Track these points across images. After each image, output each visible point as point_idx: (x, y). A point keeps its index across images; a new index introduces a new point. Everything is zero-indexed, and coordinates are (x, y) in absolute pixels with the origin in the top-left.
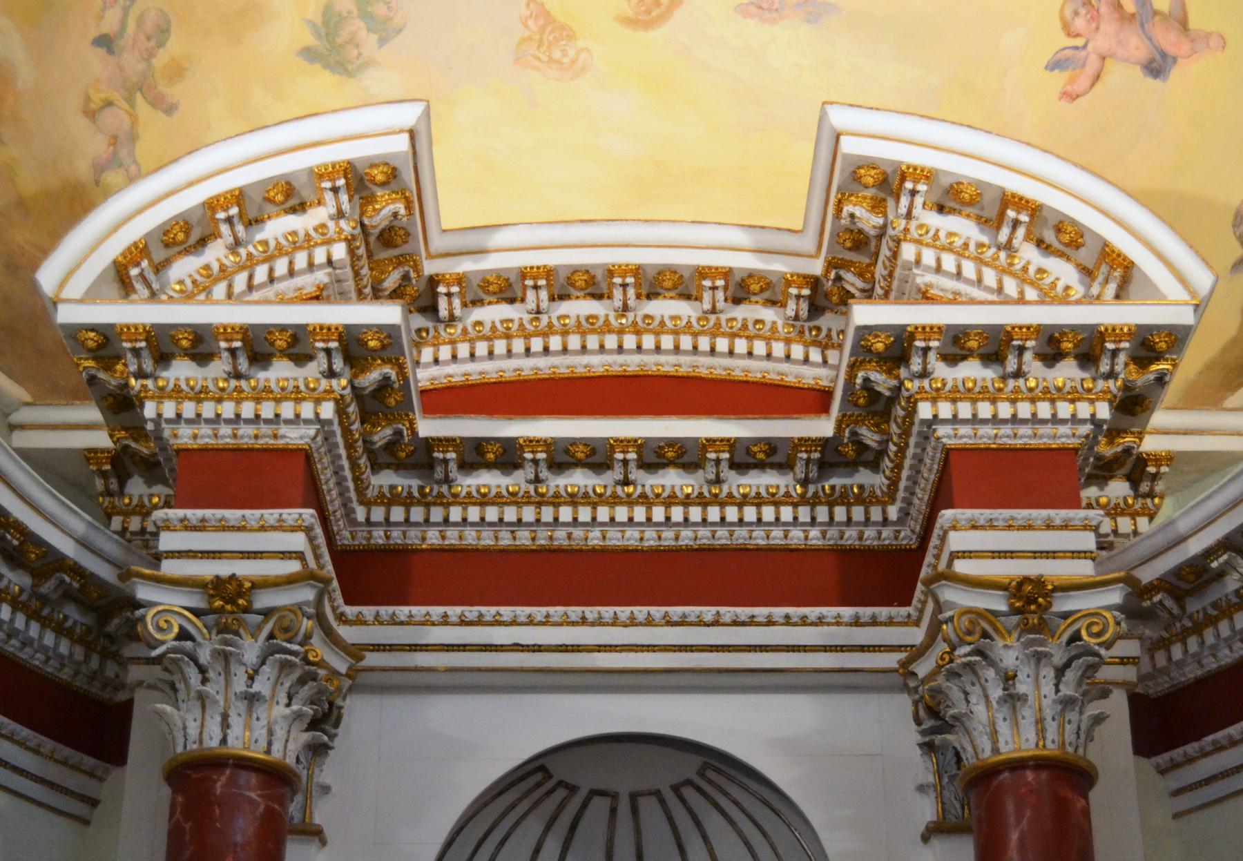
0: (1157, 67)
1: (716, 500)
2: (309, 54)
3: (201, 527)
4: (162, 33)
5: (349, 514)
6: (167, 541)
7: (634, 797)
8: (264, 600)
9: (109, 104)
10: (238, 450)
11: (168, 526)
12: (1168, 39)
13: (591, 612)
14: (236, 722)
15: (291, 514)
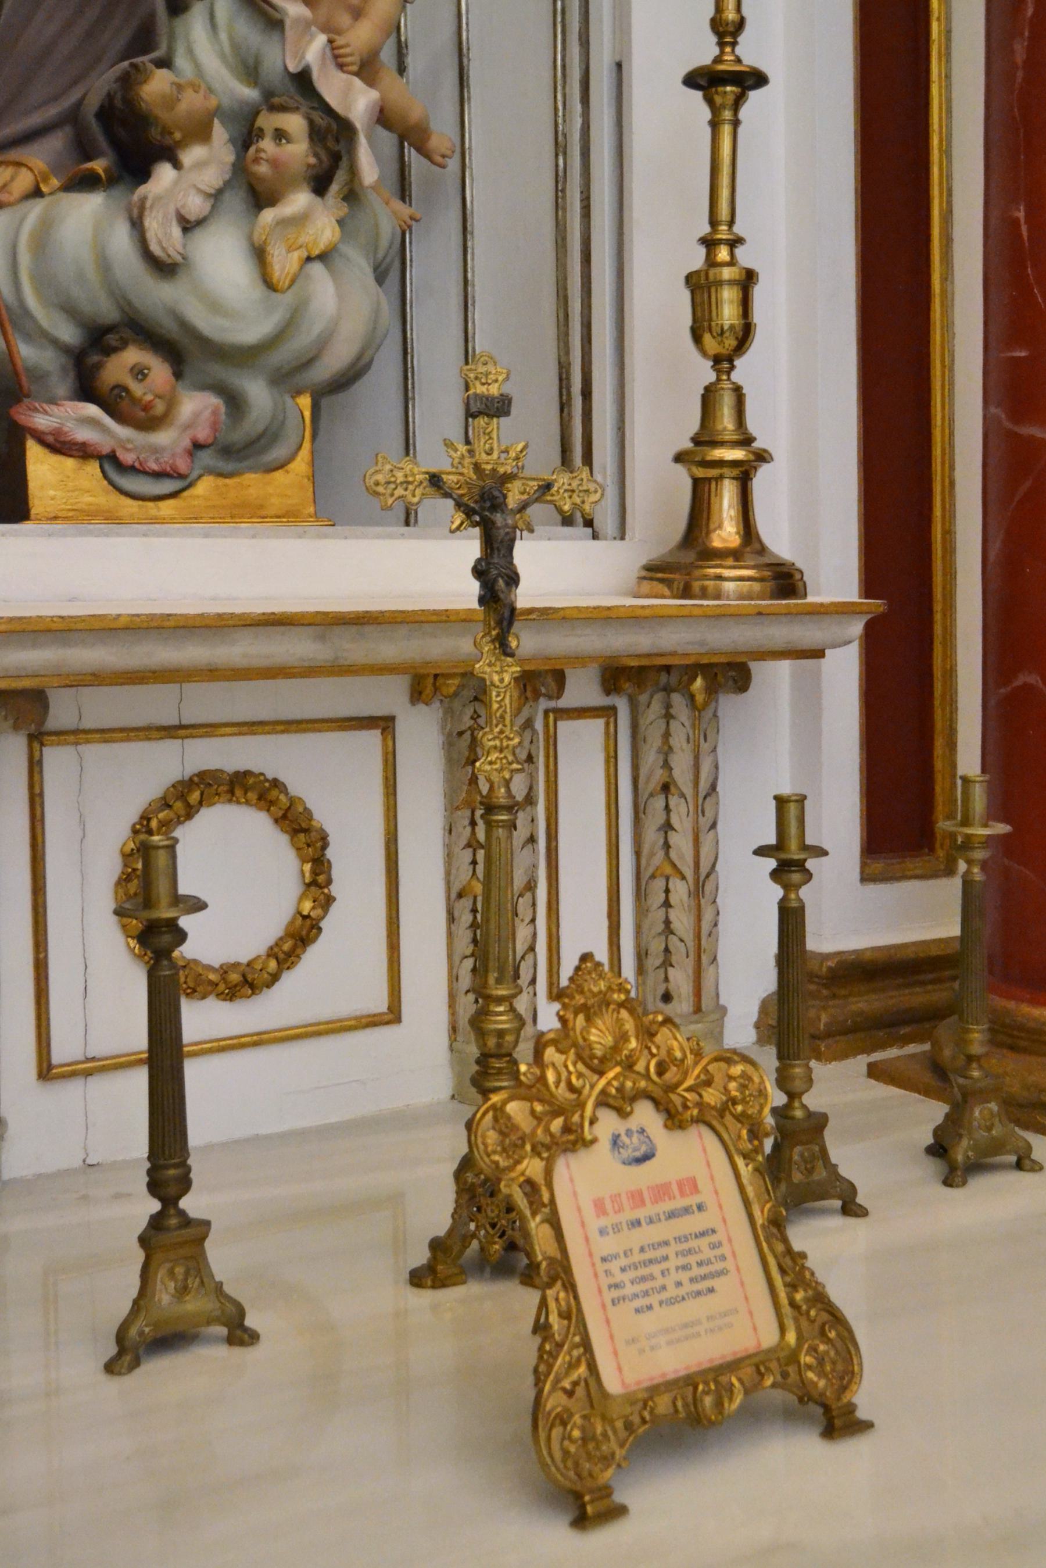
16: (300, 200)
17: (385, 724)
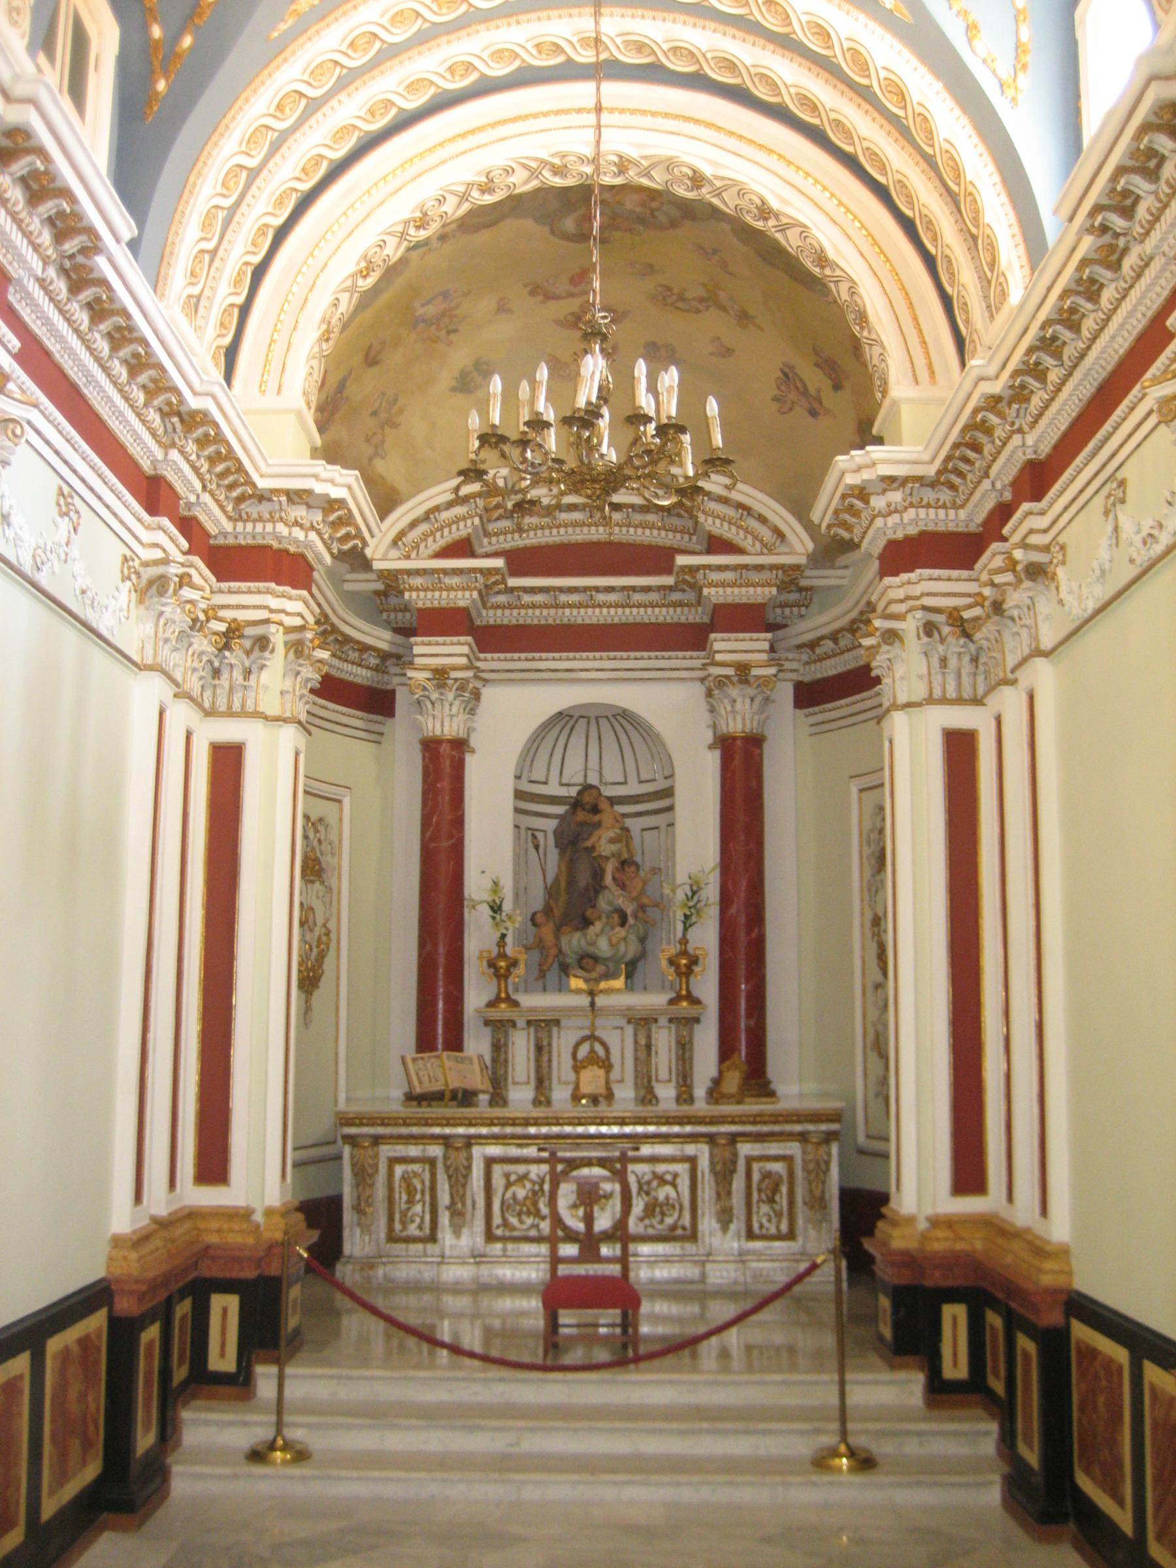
0: (813, 413)
1: (628, 606)
2: (454, 389)
3: (429, 644)
4: (396, 400)
5: (480, 615)
6: (417, 650)
7: (597, 718)
8: (453, 675)
9: (374, 434)
10: (441, 609)
11: (416, 644)
12: (816, 406)
13: (577, 655)
14: (446, 724)
15: (463, 639)
16: (618, 929)
17: (622, 1028)
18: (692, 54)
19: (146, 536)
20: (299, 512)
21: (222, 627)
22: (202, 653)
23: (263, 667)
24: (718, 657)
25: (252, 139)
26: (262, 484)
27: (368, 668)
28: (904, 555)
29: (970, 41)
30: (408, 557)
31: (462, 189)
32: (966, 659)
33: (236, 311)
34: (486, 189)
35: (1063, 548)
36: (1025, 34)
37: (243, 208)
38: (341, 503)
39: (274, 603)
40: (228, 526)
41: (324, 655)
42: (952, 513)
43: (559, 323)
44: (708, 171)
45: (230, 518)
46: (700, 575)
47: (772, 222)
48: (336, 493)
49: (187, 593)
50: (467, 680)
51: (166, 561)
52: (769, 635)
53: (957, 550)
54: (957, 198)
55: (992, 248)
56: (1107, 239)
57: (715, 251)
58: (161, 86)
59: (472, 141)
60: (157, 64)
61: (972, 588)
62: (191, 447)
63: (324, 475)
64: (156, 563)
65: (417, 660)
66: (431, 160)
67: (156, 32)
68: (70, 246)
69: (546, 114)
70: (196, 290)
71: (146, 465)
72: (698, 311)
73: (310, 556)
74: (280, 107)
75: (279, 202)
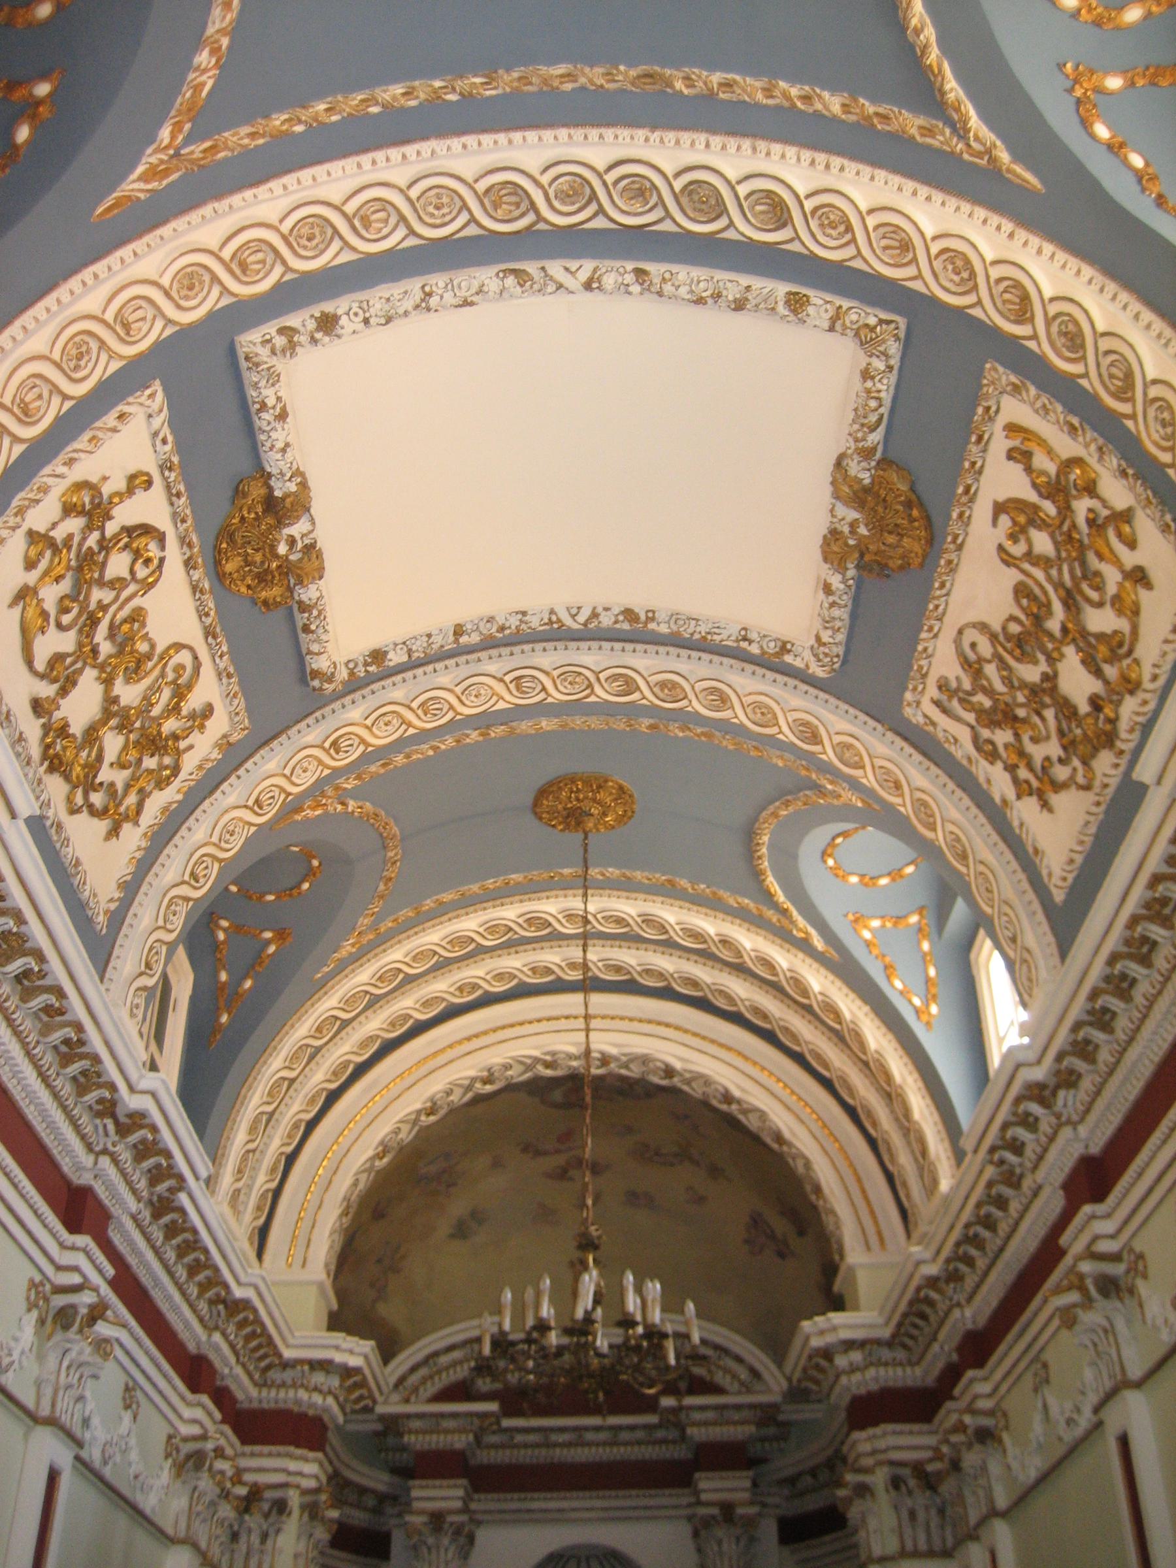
0: (781, 1255)
2: (452, 1236)
6: (415, 1493)
18: (661, 974)
19: (187, 1413)
20: (319, 1378)
21: (242, 1491)
22: (224, 1520)
23: (278, 1531)
24: (704, 1497)
25: (295, 1057)
26: (288, 1354)
27: (365, 1509)
28: (871, 1409)
29: (888, 978)
30: (407, 1401)
31: (467, 1082)
32: (933, 1512)
33: (270, 1195)
34: (486, 1081)
35: (1005, 1414)
36: (932, 972)
37: (282, 1106)
38: (357, 1370)
39: (293, 1466)
40: (254, 1392)
41: (334, 1514)
42: (908, 1370)
43: (549, 1176)
44: (678, 1065)
45: (256, 1384)
46: (683, 1416)
47: (734, 1107)
48: (354, 1361)
49: (220, 1465)
50: (462, 1524)
51: (204, 1437)
52: (751, 1473)
53: (916, 1405)
54: (892, 1095)
55: (922, 1141)
56: (1005, 1167)
57: (686, 1117)
58: (224, 1018)
59: (476, 1043)
60: (222, 1004)
61: (931, 1440)
62: (231, 1329)
63: (345, 1345)
64: (195, 1438)
65: (416, 1505)
66: (441, 1059)
67: (223, 976)
68: (161, 1188)
69: (539, 1021)
70: (240, 1184)
71: (192, 1347)
72: (672, 1165)
73: (326, 1418)
74: (319, 1029)
75: (312, 1101)
